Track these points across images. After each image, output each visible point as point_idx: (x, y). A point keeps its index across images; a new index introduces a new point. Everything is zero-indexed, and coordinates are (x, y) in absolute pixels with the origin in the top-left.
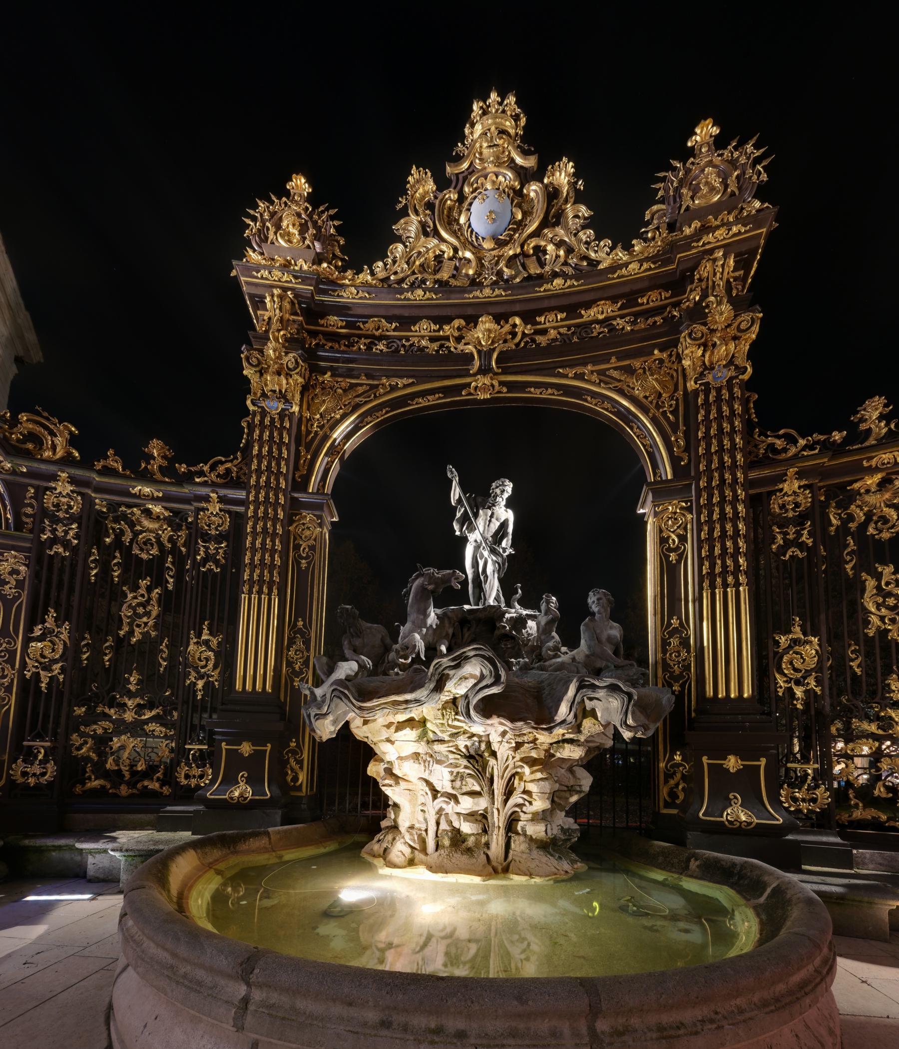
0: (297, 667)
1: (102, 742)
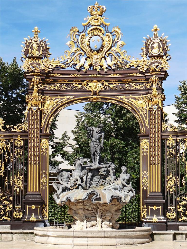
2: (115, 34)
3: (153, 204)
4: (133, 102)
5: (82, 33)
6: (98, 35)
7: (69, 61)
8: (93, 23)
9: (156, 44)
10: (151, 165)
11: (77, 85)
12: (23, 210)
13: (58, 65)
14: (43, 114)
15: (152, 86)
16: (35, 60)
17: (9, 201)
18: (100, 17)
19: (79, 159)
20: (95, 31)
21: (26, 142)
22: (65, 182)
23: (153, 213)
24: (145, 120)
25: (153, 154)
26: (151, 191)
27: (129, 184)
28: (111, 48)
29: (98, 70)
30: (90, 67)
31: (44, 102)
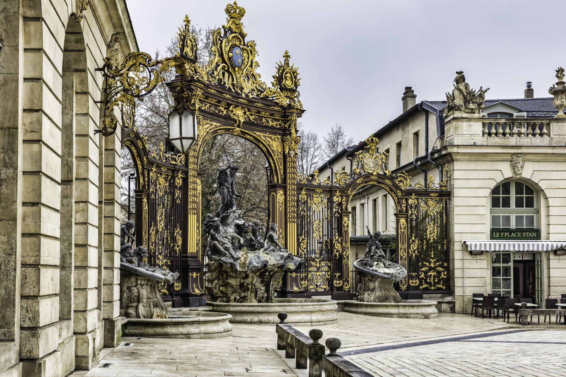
9: (288, 75)
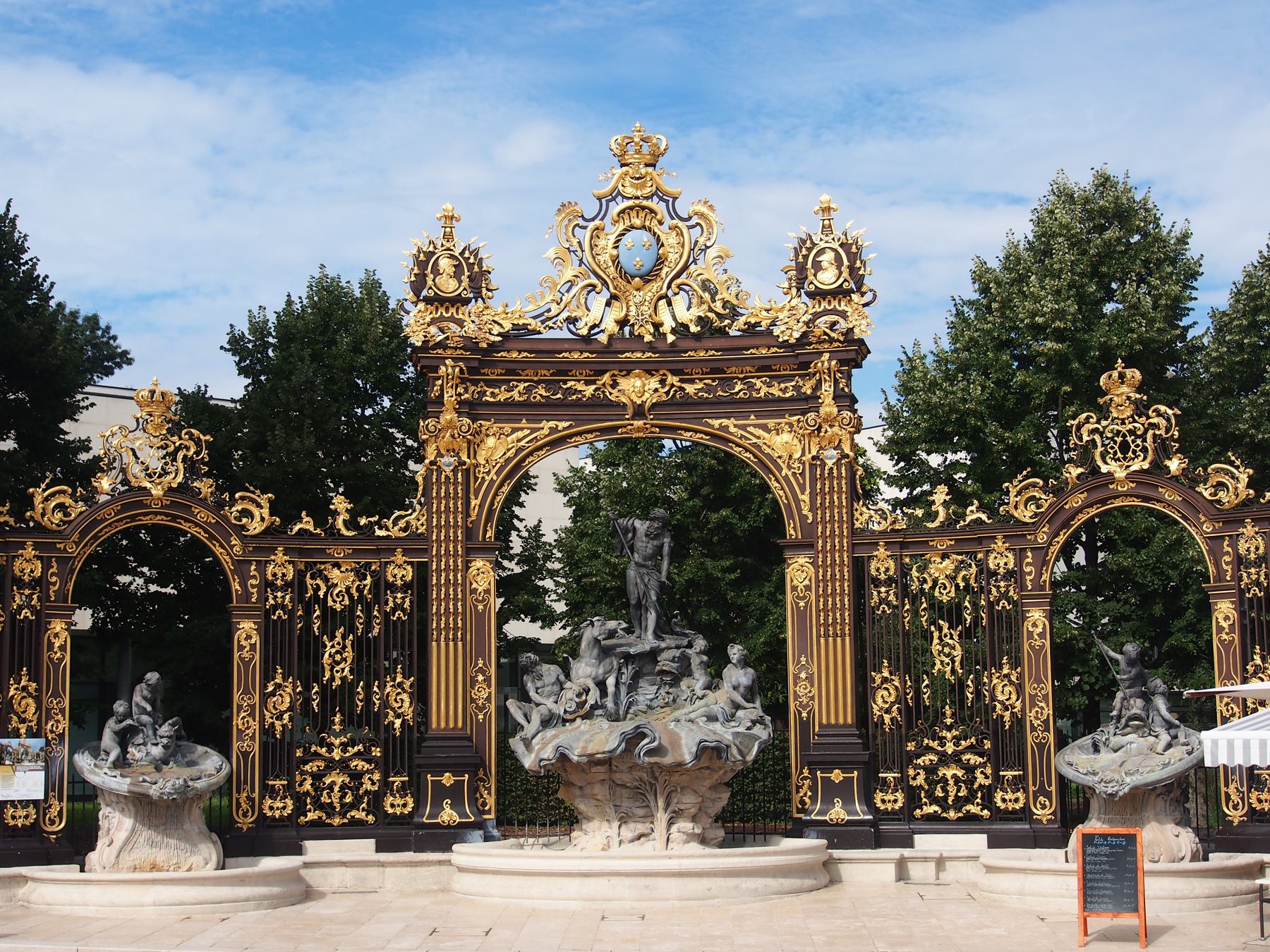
0: (480, 703)
1: (317, 777)
2: (698, 224)
3: (829, 766)
4: (759, 438)
5: (593, 219)
6: (644, 227)
7: (555, 309)
8: (630, 191)
9: (828, 257)
10: (822, 640)
11: (580, 387)
12: (415, 788)
13: (521, 322)
14: (476, 479)
15: (818, 386)
16: (447, 310)
17: (369, 762)
18: (650, 169)
19: (592, 624)
20: (633, 214)
21: (422, 571)
22: (549, 696)
23: (831, 792)
24: (801, 497)
25: (826, 603)
26: (824, 721)
27: (754, 702)
28: (686, 267)
29: (648, 338)
30: (621, 329)
31: (478, 441)
